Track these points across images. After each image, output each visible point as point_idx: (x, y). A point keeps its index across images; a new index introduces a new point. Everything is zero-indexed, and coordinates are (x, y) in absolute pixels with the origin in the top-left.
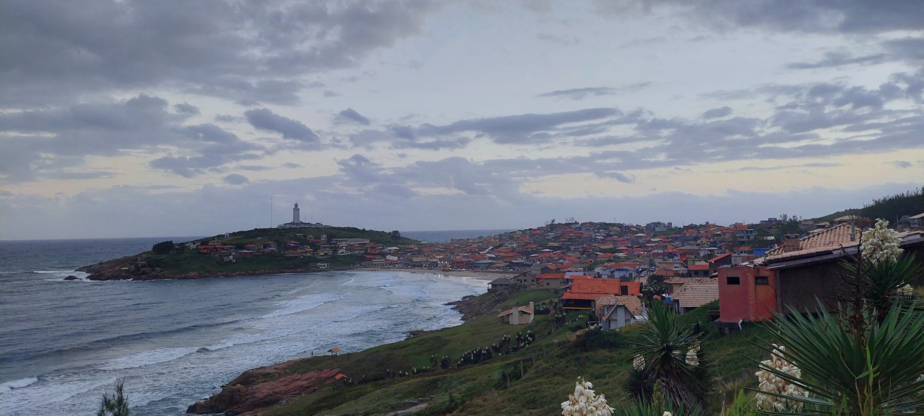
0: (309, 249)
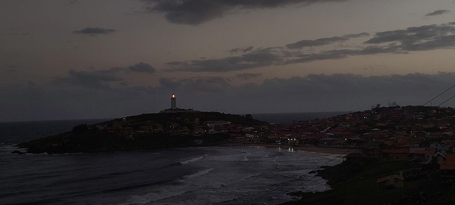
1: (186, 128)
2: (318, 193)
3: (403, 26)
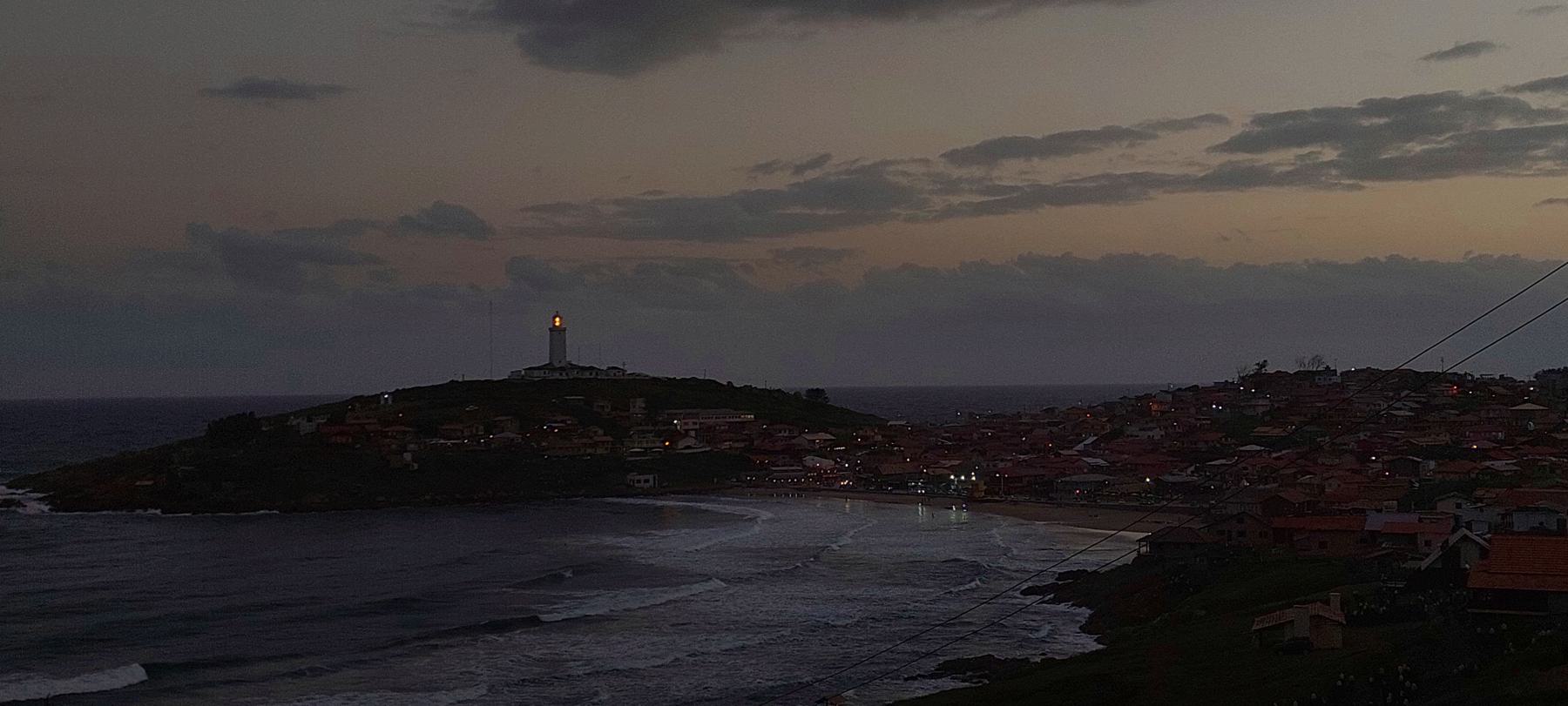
1: (601, 432)
2: (1049, 663)
3: (1350, 98)
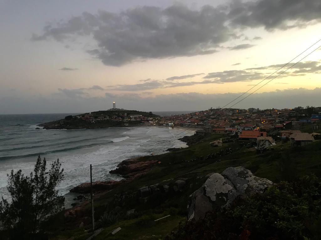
0: (120, 118)
2: (182, 149)
